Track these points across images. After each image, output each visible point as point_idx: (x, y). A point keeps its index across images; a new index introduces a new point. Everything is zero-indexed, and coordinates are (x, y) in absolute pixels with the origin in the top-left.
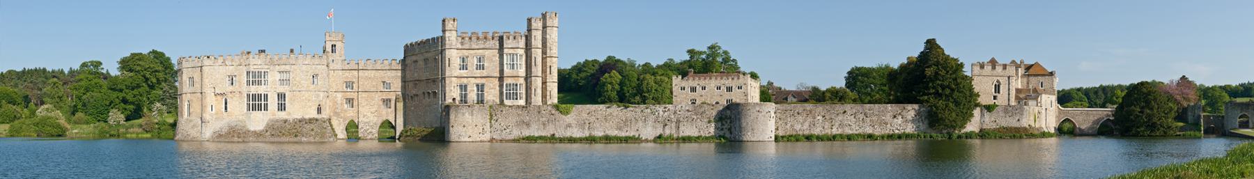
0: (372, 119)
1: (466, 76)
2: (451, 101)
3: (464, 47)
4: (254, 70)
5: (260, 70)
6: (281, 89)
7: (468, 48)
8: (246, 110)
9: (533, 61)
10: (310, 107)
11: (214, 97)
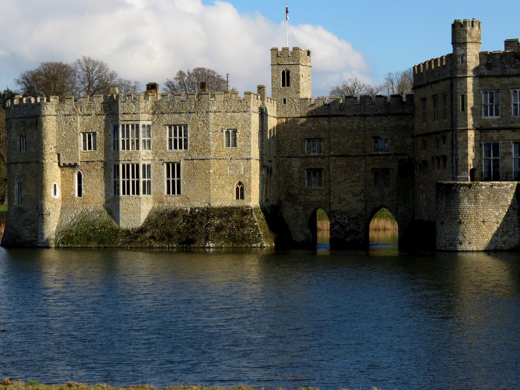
1: (495, 126)
3: (492, 72)
4: (123, 123)
7: (499, 73)
10: (223, 187)
11: (59, 170)
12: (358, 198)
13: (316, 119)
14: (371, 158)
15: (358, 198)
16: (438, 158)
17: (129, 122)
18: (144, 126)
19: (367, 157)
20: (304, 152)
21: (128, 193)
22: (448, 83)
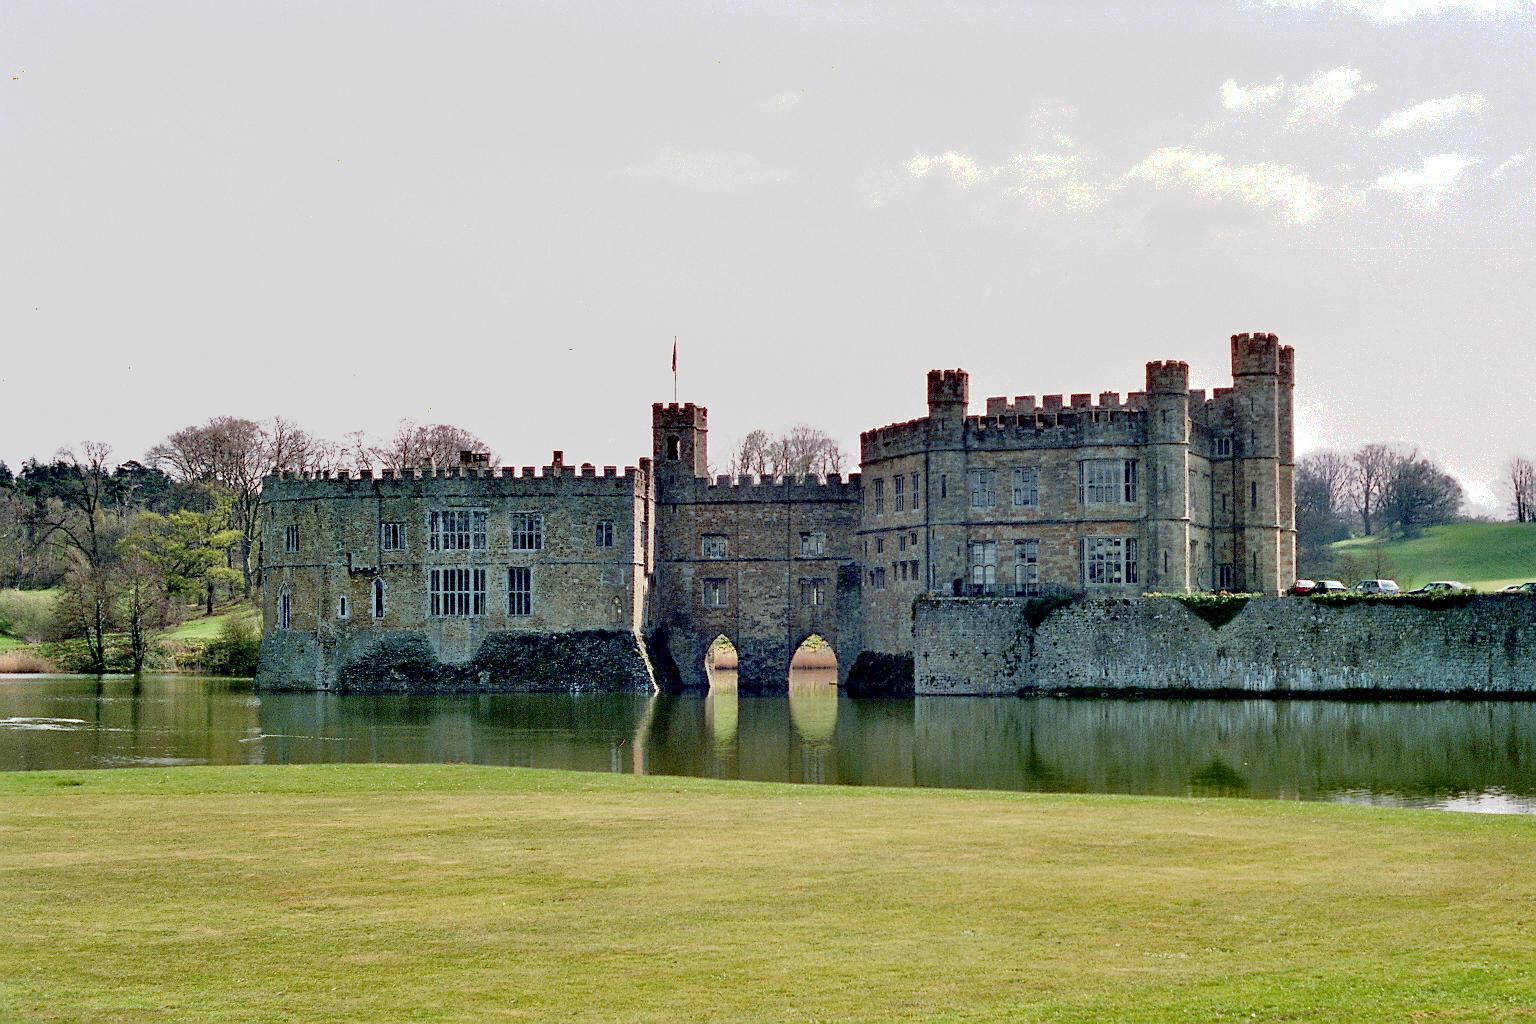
0: (773, 632)
1: (988, 519)
2: (948, 587)
3: (988, 445)
5: (465, 509)
6: (521, 557)
8: (428, 613)
9: (1159, 472)
10: (592, 603)
12: (779, 621)
13: (718, 506)
14: (799, 563)
15: (779, 621)
16: (904, 564)
17: (455, 509)
18: (476, 514)
19: (793, 562)
20: (700, 555)
21: (453, 612)
22: (923, 457)
